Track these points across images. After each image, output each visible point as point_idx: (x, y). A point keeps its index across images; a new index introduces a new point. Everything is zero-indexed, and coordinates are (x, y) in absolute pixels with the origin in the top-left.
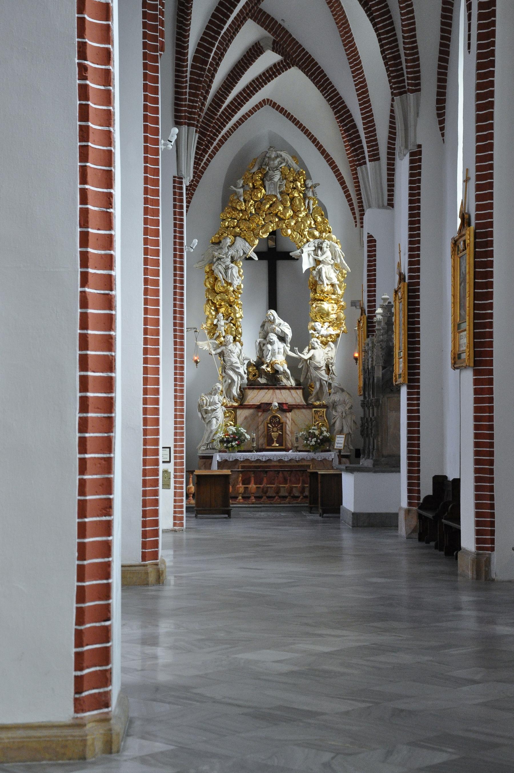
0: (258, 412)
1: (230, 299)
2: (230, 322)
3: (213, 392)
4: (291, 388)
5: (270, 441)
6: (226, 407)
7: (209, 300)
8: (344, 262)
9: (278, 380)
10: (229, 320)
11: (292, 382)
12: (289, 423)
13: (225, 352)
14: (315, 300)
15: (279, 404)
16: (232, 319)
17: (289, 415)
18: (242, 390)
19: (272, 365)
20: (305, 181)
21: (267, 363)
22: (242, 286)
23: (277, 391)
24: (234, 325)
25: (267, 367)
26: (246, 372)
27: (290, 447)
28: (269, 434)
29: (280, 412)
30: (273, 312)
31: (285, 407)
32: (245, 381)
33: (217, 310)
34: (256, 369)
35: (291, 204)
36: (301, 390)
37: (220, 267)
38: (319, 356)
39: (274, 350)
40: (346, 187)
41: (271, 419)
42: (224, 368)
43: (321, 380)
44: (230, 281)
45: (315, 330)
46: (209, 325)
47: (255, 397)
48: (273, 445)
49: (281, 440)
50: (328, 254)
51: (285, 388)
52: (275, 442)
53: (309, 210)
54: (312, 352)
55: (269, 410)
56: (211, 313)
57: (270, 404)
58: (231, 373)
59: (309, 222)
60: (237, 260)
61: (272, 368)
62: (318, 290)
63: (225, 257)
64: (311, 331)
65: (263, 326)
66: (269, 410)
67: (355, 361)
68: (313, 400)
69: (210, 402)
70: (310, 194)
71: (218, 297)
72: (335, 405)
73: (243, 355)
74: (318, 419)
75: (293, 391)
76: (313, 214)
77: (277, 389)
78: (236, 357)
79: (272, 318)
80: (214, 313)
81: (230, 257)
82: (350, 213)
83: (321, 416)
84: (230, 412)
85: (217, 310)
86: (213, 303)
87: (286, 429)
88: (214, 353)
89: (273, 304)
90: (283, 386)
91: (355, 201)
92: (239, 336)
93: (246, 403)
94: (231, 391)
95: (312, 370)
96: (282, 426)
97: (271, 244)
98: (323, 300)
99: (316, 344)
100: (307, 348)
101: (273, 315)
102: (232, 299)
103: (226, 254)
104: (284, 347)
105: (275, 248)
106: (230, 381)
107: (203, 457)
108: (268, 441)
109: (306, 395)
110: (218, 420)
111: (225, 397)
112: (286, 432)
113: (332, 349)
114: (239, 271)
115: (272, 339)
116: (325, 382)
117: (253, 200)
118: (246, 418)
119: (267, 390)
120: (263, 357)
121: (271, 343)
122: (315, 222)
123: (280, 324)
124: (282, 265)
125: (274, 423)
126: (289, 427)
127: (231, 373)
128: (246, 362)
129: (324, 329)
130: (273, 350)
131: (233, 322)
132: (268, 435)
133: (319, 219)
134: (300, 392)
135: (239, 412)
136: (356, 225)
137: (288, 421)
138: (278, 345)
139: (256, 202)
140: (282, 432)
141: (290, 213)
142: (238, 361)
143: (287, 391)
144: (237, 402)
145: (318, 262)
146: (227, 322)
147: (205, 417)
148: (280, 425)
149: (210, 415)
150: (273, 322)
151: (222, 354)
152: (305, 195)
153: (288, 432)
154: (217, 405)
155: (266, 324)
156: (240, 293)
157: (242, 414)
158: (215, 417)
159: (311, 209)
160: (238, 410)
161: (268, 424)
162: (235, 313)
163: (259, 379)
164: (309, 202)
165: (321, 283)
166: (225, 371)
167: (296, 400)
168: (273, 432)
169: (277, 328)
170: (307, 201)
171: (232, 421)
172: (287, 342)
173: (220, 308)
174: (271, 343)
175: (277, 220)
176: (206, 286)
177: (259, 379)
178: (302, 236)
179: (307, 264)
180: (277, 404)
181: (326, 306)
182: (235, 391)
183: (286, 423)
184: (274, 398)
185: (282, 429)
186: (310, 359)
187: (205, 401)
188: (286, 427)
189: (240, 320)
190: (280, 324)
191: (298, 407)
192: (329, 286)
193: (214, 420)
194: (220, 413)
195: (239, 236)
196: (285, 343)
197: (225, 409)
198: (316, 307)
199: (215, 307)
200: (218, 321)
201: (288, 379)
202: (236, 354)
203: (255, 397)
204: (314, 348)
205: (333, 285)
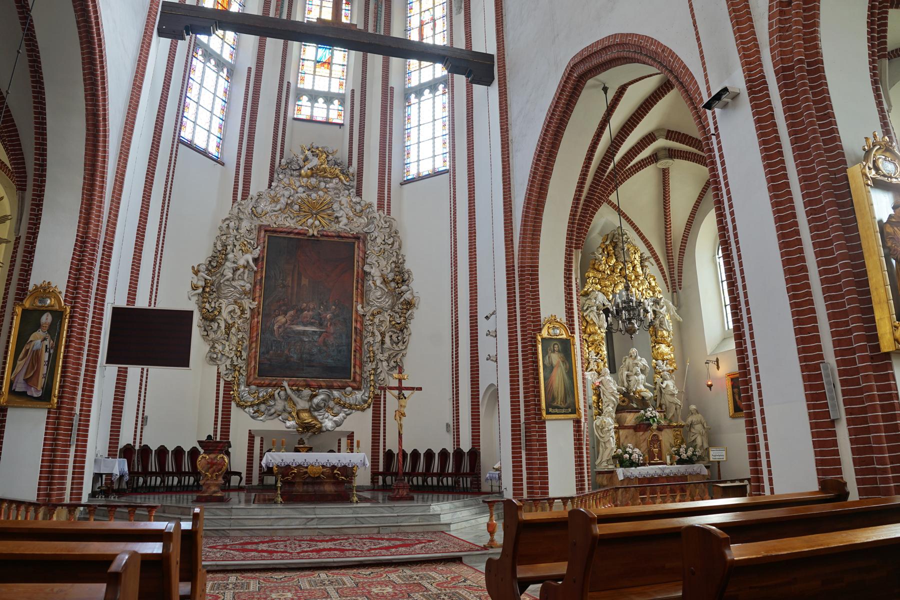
43: (676, 404)
62: (660, 333)
72: (691, 425)
91: (667, 274)
133: (653, 284)
135: (621, 432)
138: (642, 377)
152: (641, 262)
174: (636, 374)
181: (663, 348)
185: (660, 446)
203: (630, 419)
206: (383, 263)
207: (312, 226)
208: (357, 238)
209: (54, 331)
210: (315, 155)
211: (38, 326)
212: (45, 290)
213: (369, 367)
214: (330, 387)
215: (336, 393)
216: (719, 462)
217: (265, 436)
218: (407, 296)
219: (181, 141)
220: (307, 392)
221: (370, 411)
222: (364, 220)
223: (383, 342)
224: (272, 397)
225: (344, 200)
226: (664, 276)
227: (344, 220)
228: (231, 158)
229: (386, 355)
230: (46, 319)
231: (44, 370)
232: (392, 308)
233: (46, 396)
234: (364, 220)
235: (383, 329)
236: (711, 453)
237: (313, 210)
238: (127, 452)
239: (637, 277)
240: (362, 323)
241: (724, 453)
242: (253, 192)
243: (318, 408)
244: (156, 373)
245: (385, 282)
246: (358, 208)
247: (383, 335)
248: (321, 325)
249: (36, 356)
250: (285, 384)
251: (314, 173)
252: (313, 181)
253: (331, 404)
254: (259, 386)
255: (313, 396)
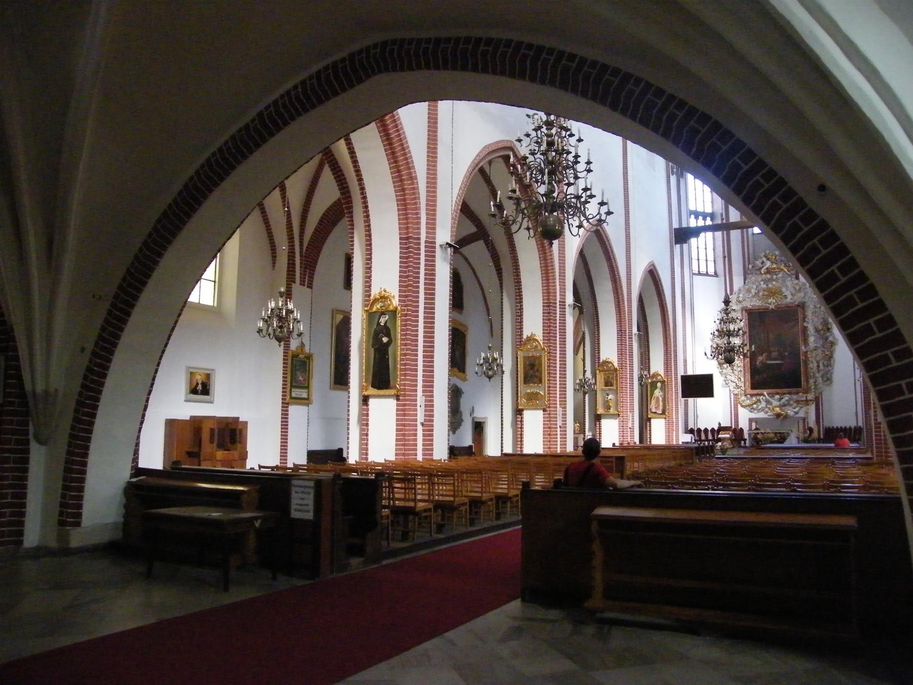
206: (816, 319)
207: (772, 303)
208: (798, 306)
209: (663, 389)
210: (768, 259)
211: (656, 388)
212: (656, 375)
213: (811, 381)
214: (790, 393)
215: (795, 397)
217: (756, 420)
218: (831, 339)
219: (694, 274)
220: (777, 397)
221: (814, 405)
222: (802, 294)
223: (818, 366)
224: (759, 401)
225: (789, 284)
227: (790, 297)
228: (720, 271)
229: (821, 373)
230: (659, 385)
231: (661, 403)
232: (823, 346)
233: (664, 412)
234: (802, 294)
235: (818, 359)
237: (771, 293)
238: (691, 431)
240: (806, 357)
242: (736, 288)
243: (784, 405)
244: (702, 401)
245: (817, 330)
246: (797, 288)
247: (818, 362)
248: (782, 360)
249: (658, 399)
250: (765, 393)
251: (768, 271)
252: (769, 276)
253: (791, 402)
254: (752, 395)
255: (780, 399)
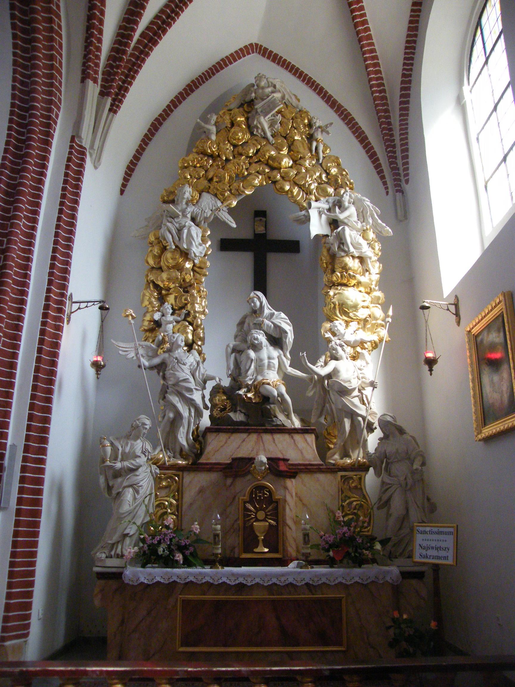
0: (226, 477)
1: (184, 280)
2: (185, 320)
3: (134, 432)
4: (295, 431)
5: (250, 542)
6: (162, 467)
7: (148, 283)
8: (380, 221)
9: (268, 416)
10: (183, 317)
11: (297, 424)
12: (291, 501)
13: (168, 362)
14: (333, 285)
15: (268, 459)
16: (188, 314)
17: (290, 483)
18: (200, 438)
19: (257, 387)
20: (310, 121)
21: (247, 386)
22: (208, 264)
23: (267, 437)
24: (191, 324)
25: (249, 391)
26: (209, 405)
27: (294, 554)
28: (248, 525)
29: (271, 477)
30: (260, 294)
31: (283, 467)
32: (206, 421)
33: (162, 300)
34: (227, 399)
35: (290, 150)
36: (313, 436)
37: (169, 224)
38: (347, 371)
39: (261, 360)
40: (369, 143)
41: (251, 493)
42: (164, 392)
44: (185, 246)
45: (334, 334)
46: (146, 323)
47: (224, 448)
48: (256, 550)
49: (274, 537)
50: (352, 210)
51: (282, 430)
52: (261, 544)
53: (318, 160)
54: (333, 364)
55: (249, 472)
56: (151, 303)
57: (251, 460)
58: (175, 400)
59: (318, 174)
60: (200, 222)
61: (257, 393)
63: (180, 214)
64: (328, 335)
65: (241, 324)
66: (249, 472)
67: (426, 368)
68: (337, 456)
69: (123, 453)
70: (319, 136)
71: (164, 276)
73: (202, 371)
74: (350, 494)
75: (297, 437)
76: (323, 165)
77: (266, 431)
78: (188, 372)
79: (258, 304)
80: (156, 303)
81: (189, 216)
82: (377, 177)
83: (356, 487)
84: (170, 478)
85: (162, 300)
86: (156, 286)
87: (284, 515)
88: (145, 362)
89: (260, 283)
90: (277, 425)
92: (199, 343)
93: (202, 460)
94: (176, 438)
95: (333, 396)
96: (276, 509)
97: (260, 229)
98: (346, 285)
99: (339, 349)
100: (322, 359)
101: (259, 298)
102: (188, 278)
103: (184, 211)
104: (279, 357)
105: (265, 233)
106: (171, 415)
107: (101, 576)
108: (244, 540)
109: (323, 450)
110: (137, 492)
111: (161, 450)
112: (285, 524)
113: (367, 363)
114: (204, 241)
115: (257, 339)
116: (360, 419)
117: (231, 144)
118: (201, 491)
119: (244, 435)
120: (240, 374)
121: (257, 348)
122: (328, 174)
123: (272, 315)
124: (276, 263)
125: (260, 502)
126: (291, 510)
127: (175, 400)
128: (210, 385)
129: (351, 332)
130: (260, 360)
131: (189, 319)
132: (245, 528)
133: (334, 171)
134: (311, 438)
136: (387, 193)
137: (288, 498)
138: (268, 352)
139: (235, 146)
140: (277, 521)
141: (287, 162)
142: (191, 379)
143: (287, 436)
144: (185, 459)
145: (334, 223)
146: (179, 319)
147: (111, 483)
148: (274, 507)
149: (119, 480)
150: (257, 312)
151: (161, 367)
153: (289, 522)
154: (138, 460)
155: (247, 320)
156: (205, 275)
157: (195, 482)
158: (131, 486)
159: (321, 155)
160: (185, 474)
161: (245, 502)
162: (193, 304)
163: (231, 414)
164: (316, 148)
165: (343, 254)
166: (165, 397)
167: (305, 453)
168: (257, 520)
169: (266, 322)
170: (314, 144)
171: (174, 497)
172: (285, 347)
173: (167, 295)
175: (267, 170)
176: (148, 263)
177: (231, 414)
178: (307, 194)
179: (317, 226)
180: (265, 460)
181: (351, 295)
182: (183, 438)
183: (285, 501)
184: (262, 449)
186: (329, 376)
187: (109, 449)
188: (284, 509)
189: (203, 317)
190: (272, 315)
191: (308, 469)
192: (357, 261)
193: (129, 494)
194: (145, 478)
195: (208, 192)
196: (282, 349)
197: (158, 471)
198: (335, 294)
199: (160, 293)
200: (163, 315)
201: (288, 416)
202: (187, 366)
204: (337, 359)
205: (362, 260)
216: (436, 568)
226: (378, 166)
236: (419, 539)
239: (297, 162)
241: (449, 541)
